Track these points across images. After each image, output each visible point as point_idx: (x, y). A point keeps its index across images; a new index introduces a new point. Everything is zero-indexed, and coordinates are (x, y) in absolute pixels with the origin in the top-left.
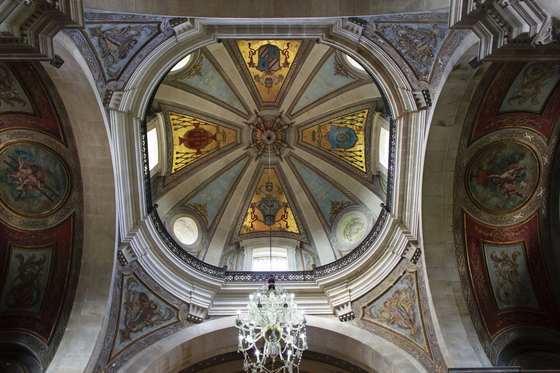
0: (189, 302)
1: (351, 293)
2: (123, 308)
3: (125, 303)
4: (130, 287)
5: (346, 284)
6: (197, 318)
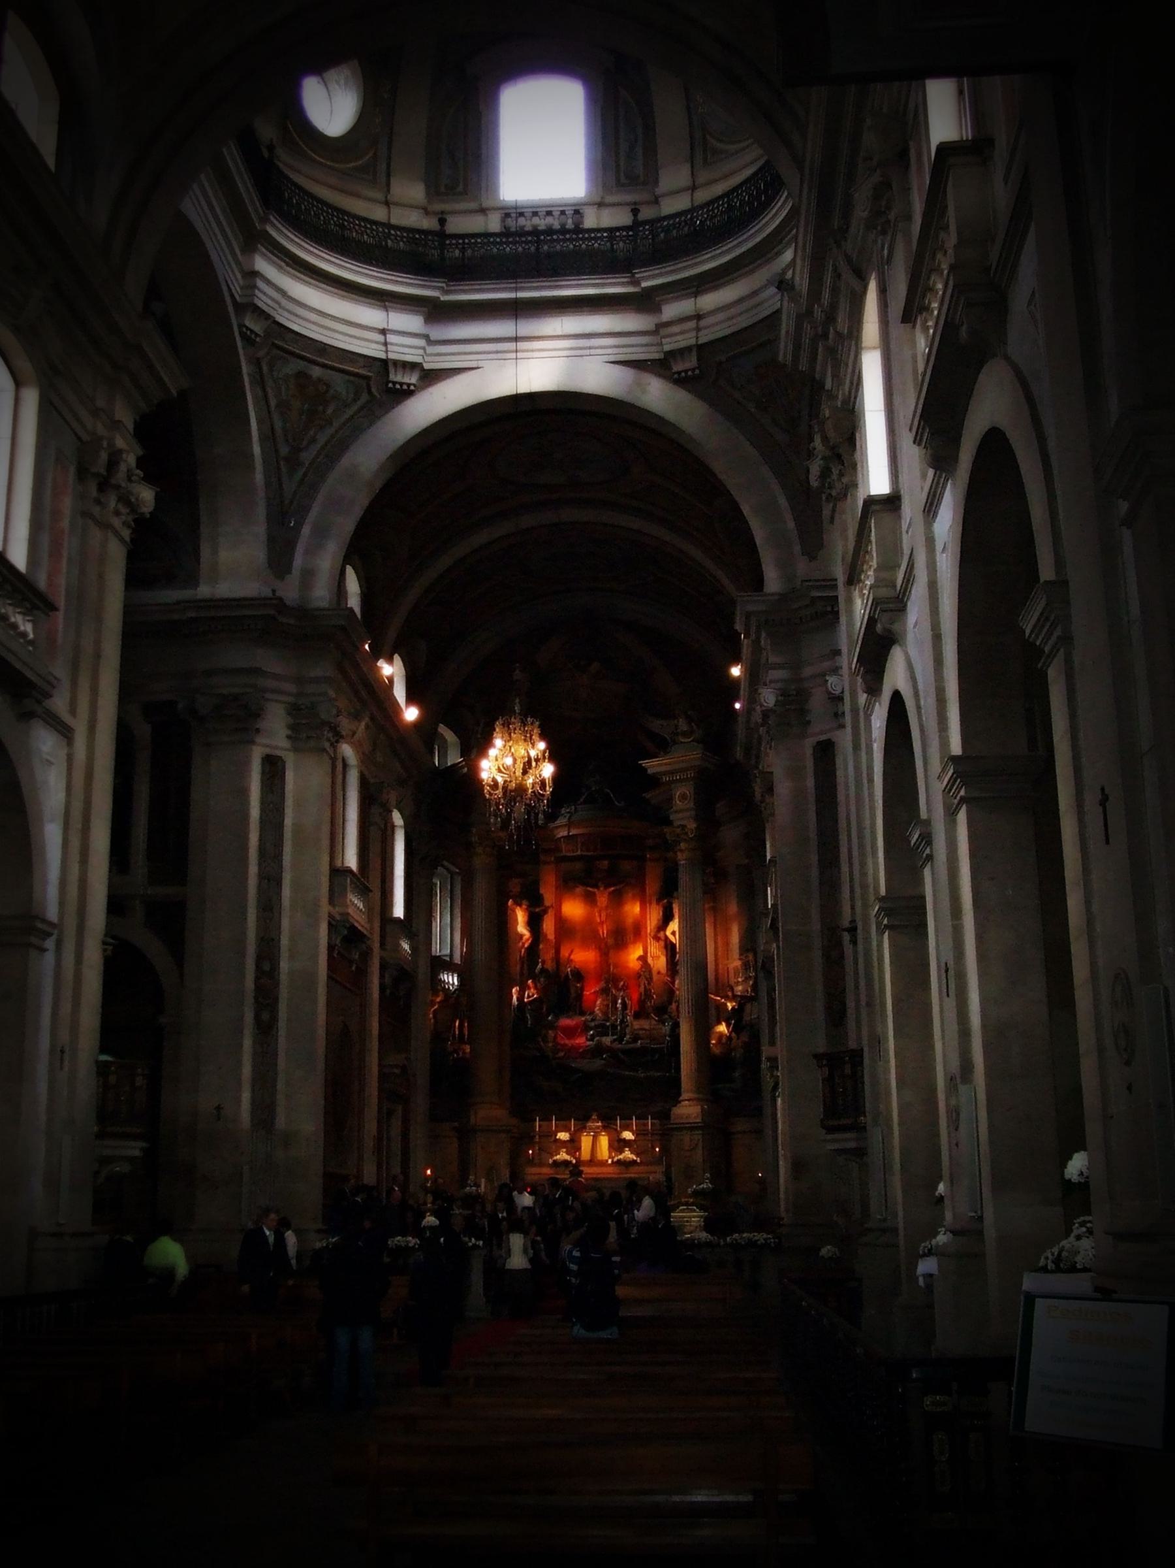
0: (383, 356)
1: (703, 323)
2: (276, 417)
3: (277, 406)
4: (275, 373)
5: (694, 289)
6: (405, 387)
